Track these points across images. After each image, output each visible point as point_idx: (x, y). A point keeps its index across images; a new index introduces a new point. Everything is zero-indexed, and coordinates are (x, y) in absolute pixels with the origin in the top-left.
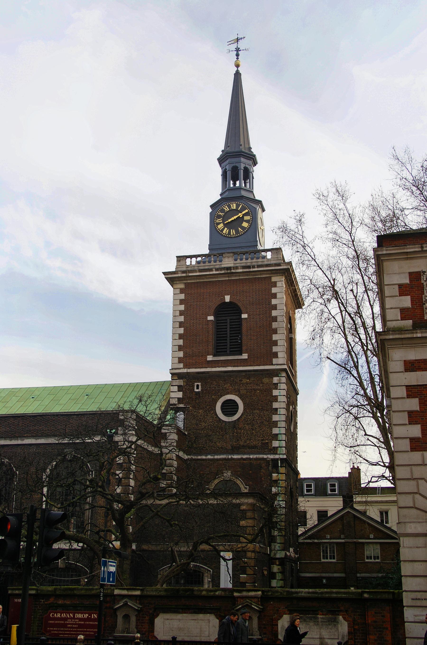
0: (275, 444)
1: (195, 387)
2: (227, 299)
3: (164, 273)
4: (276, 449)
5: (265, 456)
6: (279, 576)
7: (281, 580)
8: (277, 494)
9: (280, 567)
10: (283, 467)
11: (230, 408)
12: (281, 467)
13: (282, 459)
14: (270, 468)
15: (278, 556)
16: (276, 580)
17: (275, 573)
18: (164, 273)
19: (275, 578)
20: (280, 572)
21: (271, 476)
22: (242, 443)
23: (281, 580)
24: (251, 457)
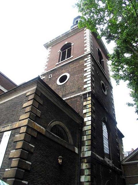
0: (85, 86)
1: (49, 77)
2: (66, 43)
3: (44, 45)
4: (85, 89)
5: (79, 94)
6: (87, 172)
7: (88, 175)
8: (86, 113)
9: (87, 164)
10: (90, 96)
11: (63, 79)
12: (88, 97)
13: (89, 93)
14: (82, 100)
15: (86, 156)
16: (85, 176)
17: (84, 170)
18: (44, 45)
19: (83, 174)
20: (88, 169)
21: (83, 104)
22: (67, 92)
23: (88, 175)
24: (71, 97)
